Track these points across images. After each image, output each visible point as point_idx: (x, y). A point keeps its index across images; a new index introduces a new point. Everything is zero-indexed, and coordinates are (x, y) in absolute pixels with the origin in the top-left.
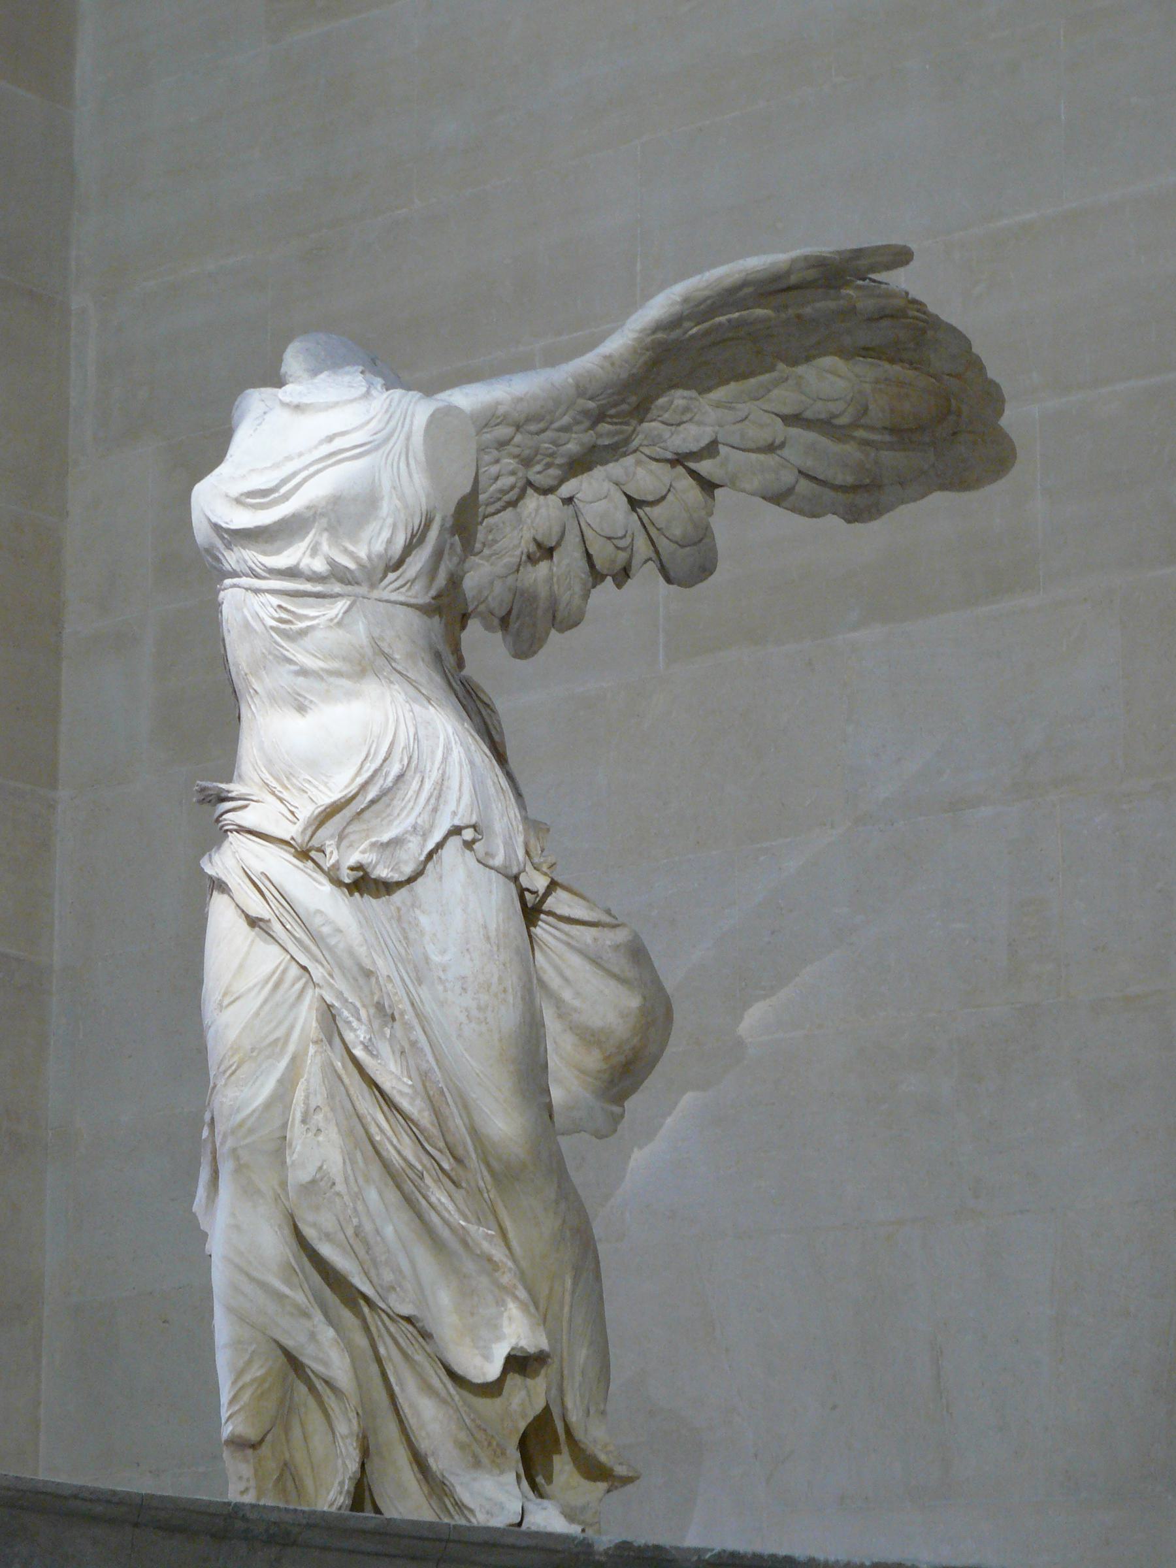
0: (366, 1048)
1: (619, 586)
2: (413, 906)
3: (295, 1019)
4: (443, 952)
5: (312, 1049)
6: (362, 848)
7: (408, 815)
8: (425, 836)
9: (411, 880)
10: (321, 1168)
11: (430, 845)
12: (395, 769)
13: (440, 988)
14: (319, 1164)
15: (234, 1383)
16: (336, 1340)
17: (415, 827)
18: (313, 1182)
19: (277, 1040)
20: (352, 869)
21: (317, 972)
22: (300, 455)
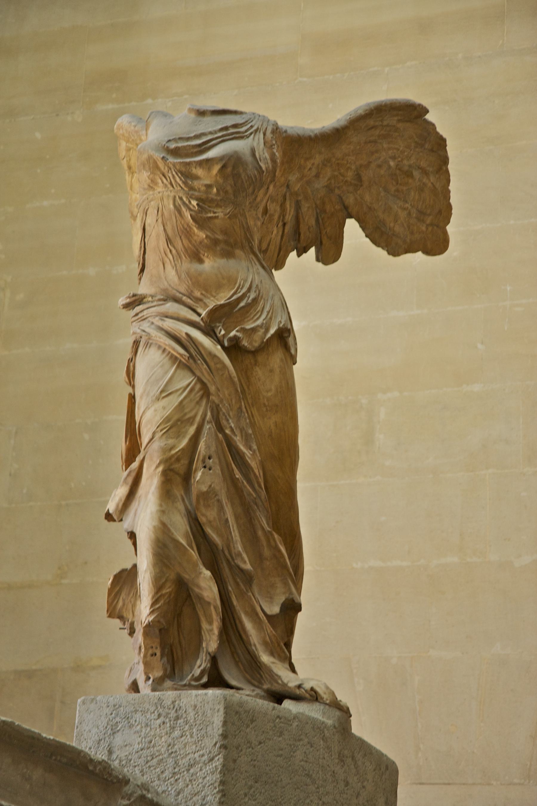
0: (232, 430)
1: (299, 255)
2: (256, 364)
3: (198, 410)
4: (267, 392)
5: (207, 427)
6: (237, 329)
7: (258, 319)
8: (267, 330)
9: (255, 353)
10: (210, 486)
11: (269, 335)
12: (252, 295)
13: (265, 409)
14: (209, 483)
15: (156, 593)
16: (211, 578)
17: (263, 324)
18: (207, 492)
19: (189, 419)
20: (230, 340)
21: (212, 389)
22: (211, 133)
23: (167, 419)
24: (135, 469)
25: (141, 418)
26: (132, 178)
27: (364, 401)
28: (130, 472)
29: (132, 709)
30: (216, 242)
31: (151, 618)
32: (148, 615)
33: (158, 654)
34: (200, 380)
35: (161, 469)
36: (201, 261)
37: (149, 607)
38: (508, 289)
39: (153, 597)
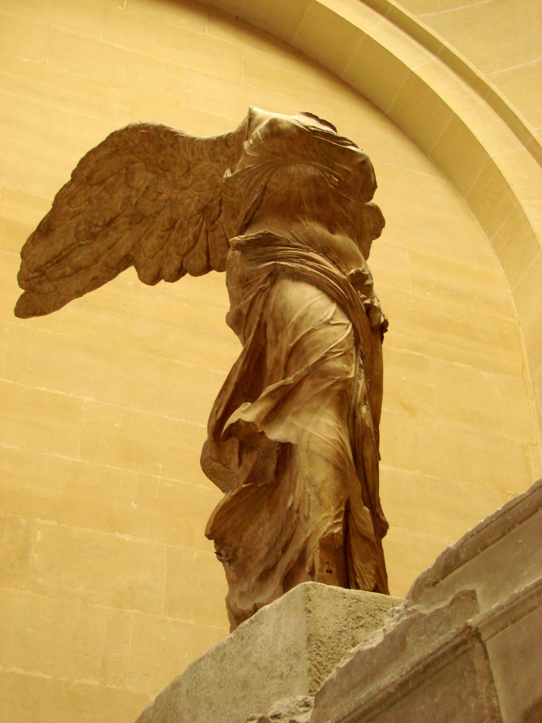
23: (340, 345)
24: (292, 384)
25: (303, 337)
26: (80, 190)
27: (23, 521)
28: (282, 386)
29: (374, 606)
30: (347, 221)
31: (336, 531)
32: (331, 527)
33: (334, 570)
34: (354, 327)
35: (339, 387)
36: (332, 232)
37: (332, 519)
38: (160, 466)
39: (337, 509)
